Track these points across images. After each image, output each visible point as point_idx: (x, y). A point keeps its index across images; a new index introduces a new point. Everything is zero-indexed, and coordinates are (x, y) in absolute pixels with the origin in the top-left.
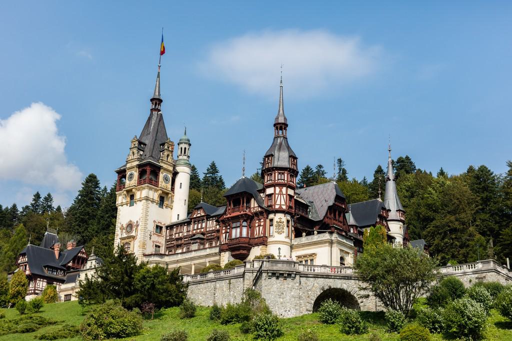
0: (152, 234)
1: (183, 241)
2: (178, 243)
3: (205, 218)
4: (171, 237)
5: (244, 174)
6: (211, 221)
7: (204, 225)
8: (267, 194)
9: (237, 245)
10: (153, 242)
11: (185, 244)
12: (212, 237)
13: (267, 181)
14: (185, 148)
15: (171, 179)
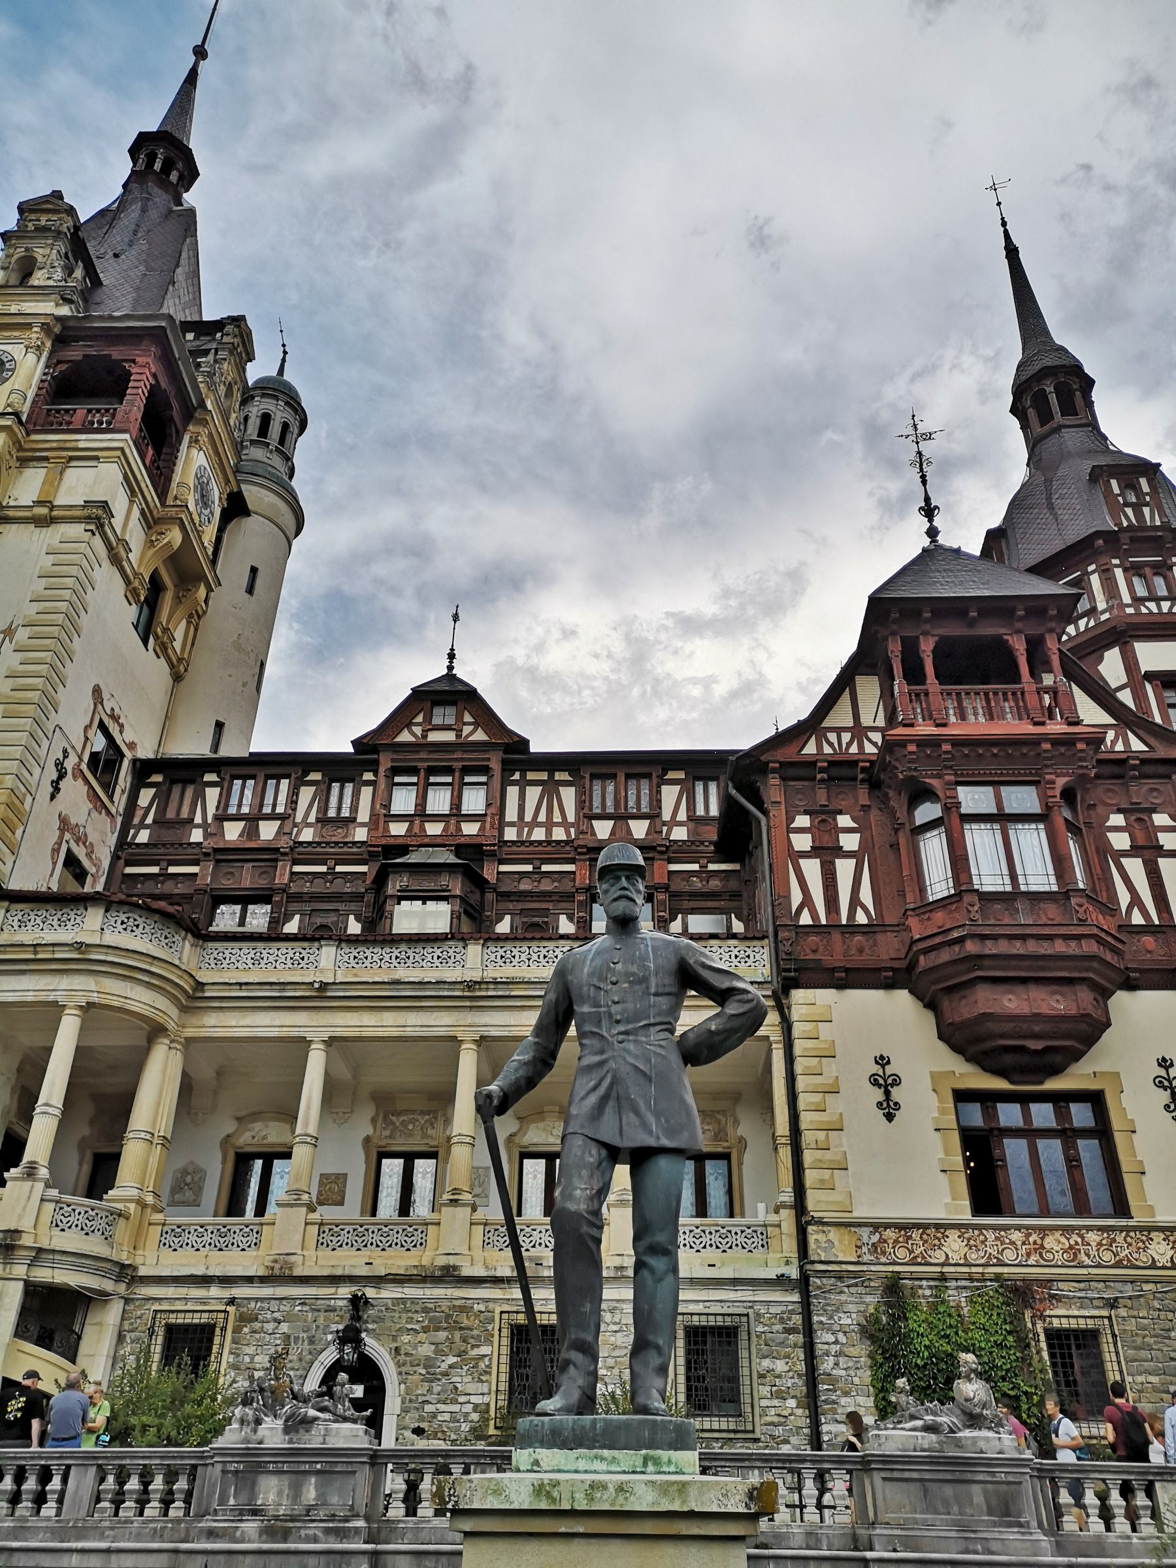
0: (69, 764)
1: (282, 876)
2: (227, 883)
3: (495, 765)
4: (168, 836)
5: (932, 533)
6: (533, 793)
7: (474, 800)
8: (1145, 666)
9: (1060, 947)
10: (64, 824)
11: (298, 898)
12: (546, 886)
13: (1137, 601)
14: (285, 427)
15: (218, 512)
